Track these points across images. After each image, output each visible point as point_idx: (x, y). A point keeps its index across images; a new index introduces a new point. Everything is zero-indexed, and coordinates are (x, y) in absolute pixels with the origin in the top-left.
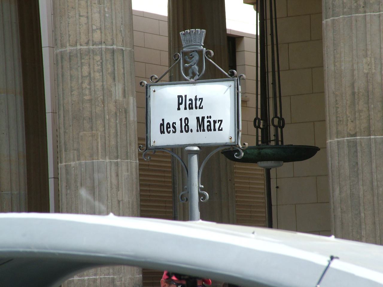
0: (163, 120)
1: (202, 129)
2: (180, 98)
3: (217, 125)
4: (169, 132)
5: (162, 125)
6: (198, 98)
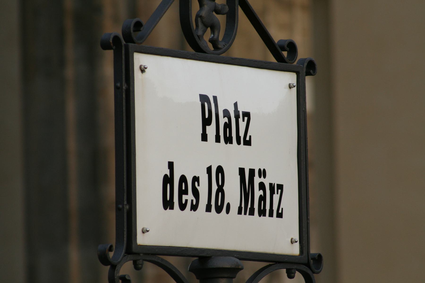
0: (171, 165)
5: (168, 180)
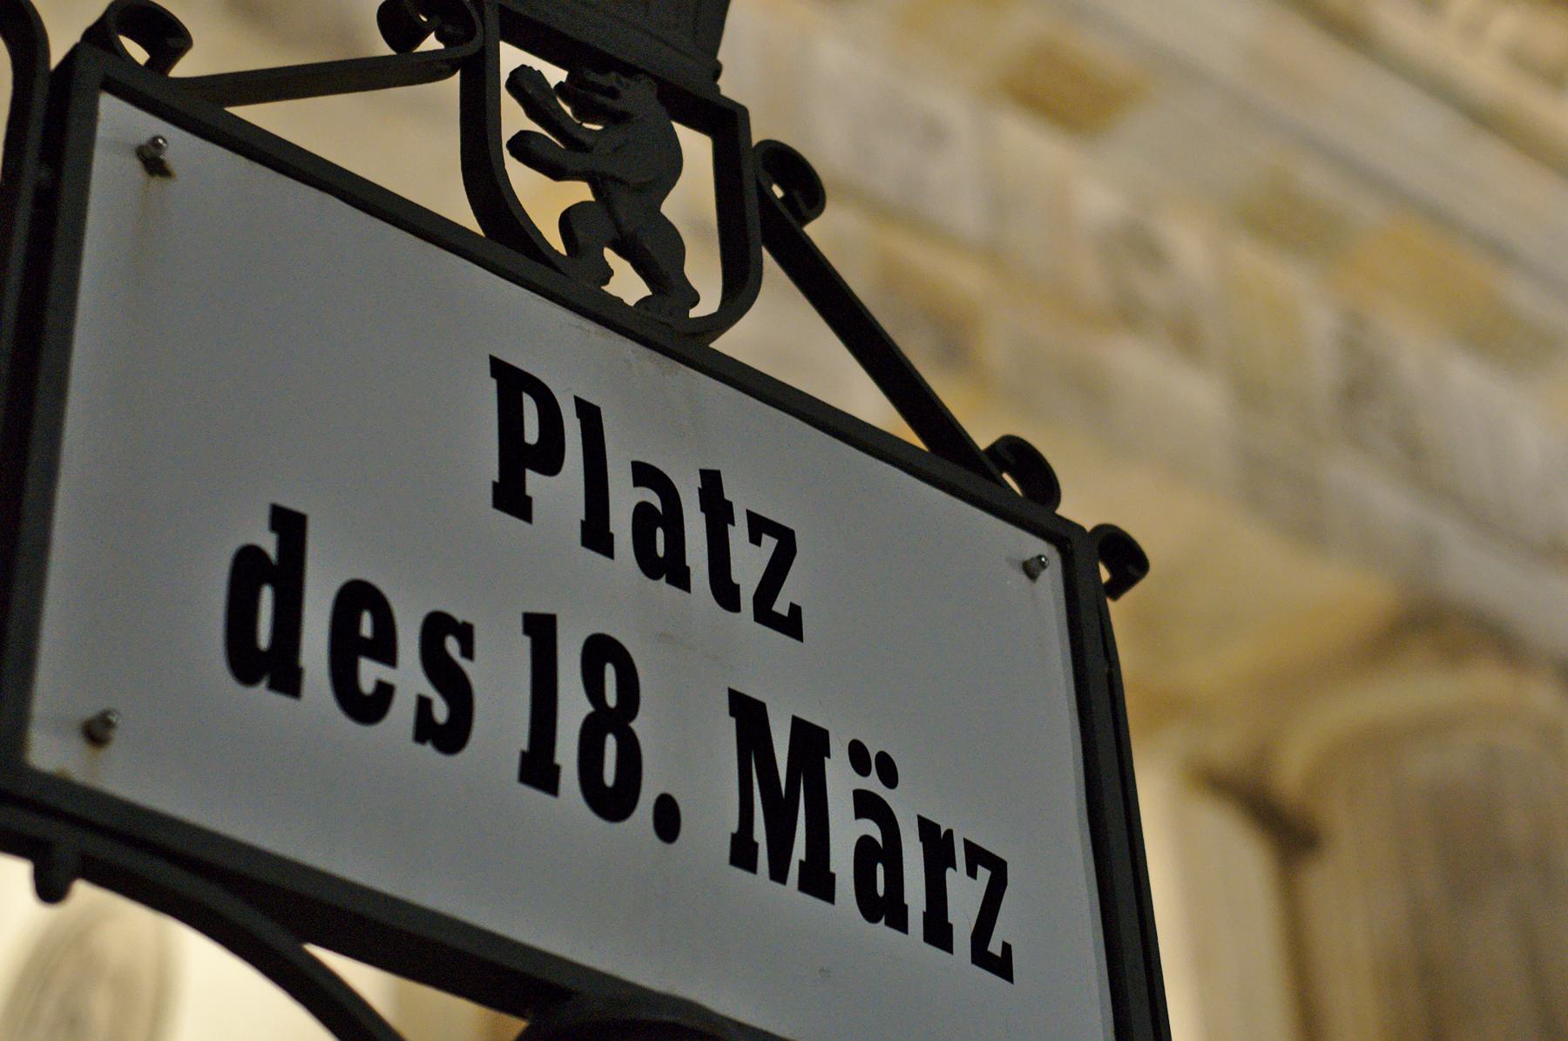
0: (289, 524)
1: (799, 851)
4: (367, 708)
5: (268, 572)
6: (740, 497)
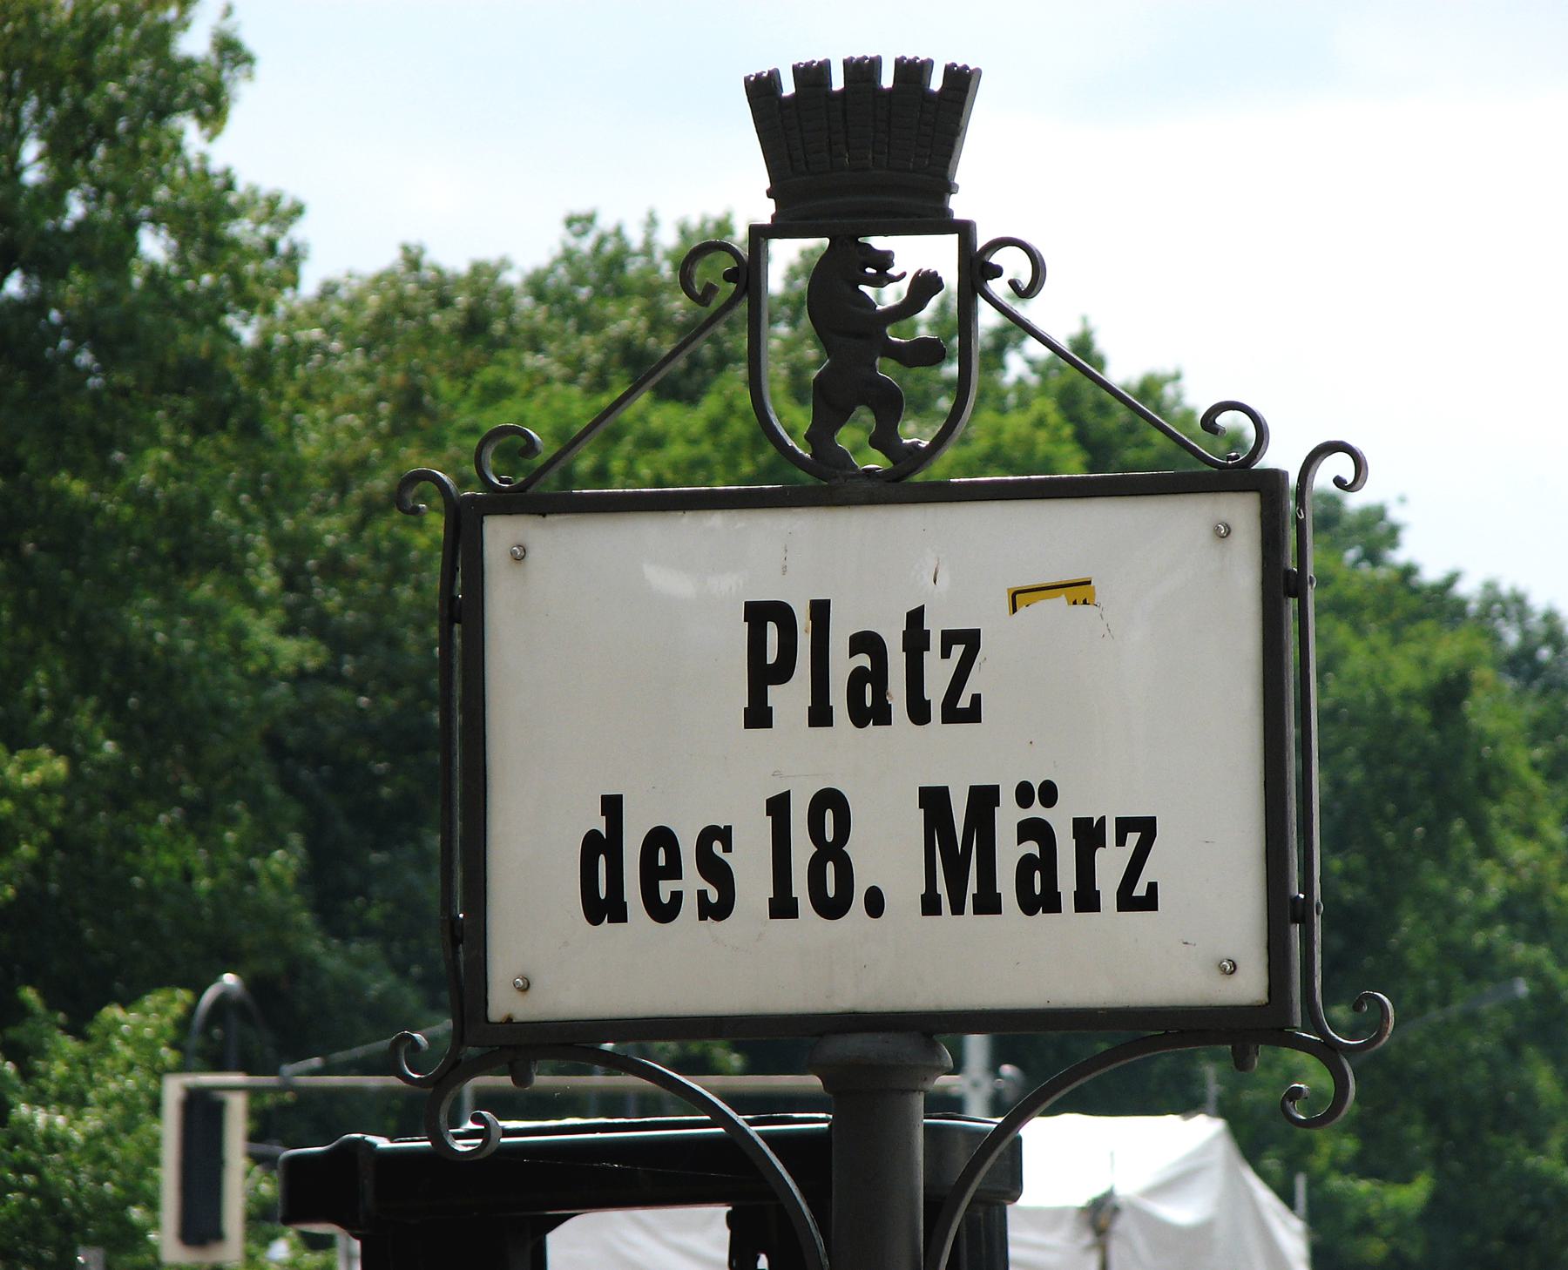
0: (612, 806)
1: (972, 887)
2: (772, 630)
3: (1111, 863)
4: (664, 912)
5: (601, 847)
6: (934, 626)
